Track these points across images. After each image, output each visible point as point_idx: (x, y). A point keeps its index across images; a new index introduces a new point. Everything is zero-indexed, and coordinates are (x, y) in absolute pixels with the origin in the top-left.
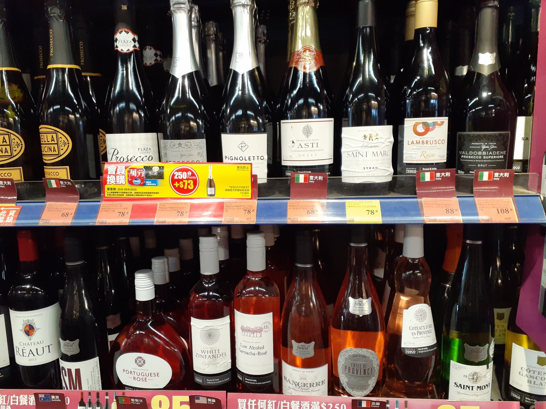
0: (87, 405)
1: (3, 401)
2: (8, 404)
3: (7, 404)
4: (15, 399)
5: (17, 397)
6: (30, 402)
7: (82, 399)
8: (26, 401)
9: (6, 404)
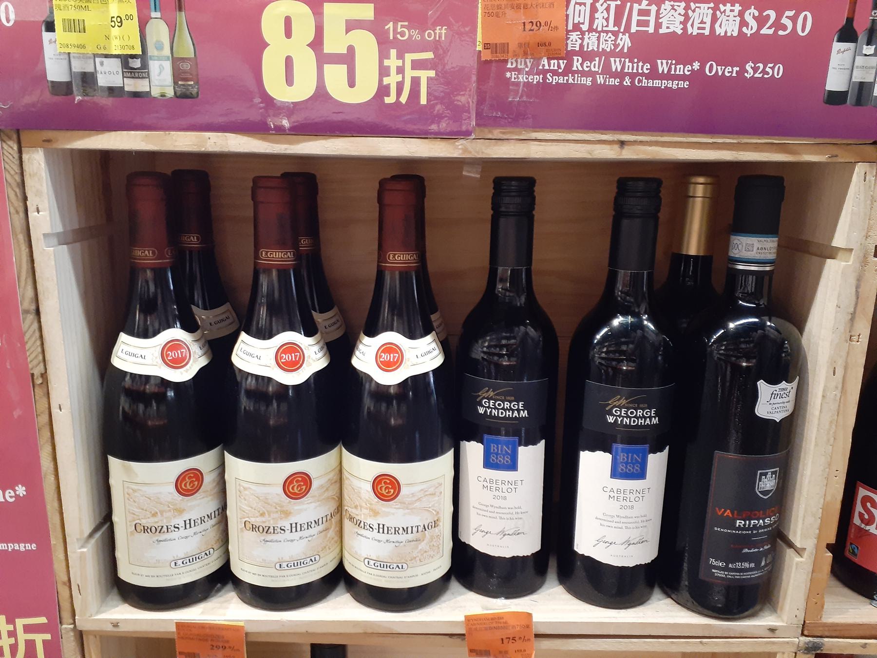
0: (862, 37)
1: (607, 20)
2: (622, 30)
3: (619, 27)
4: (647, 13)
5: (654, 8)
6: (692, 25)
7: (850, 20)
8: (677, 23)
9: (616, 29)
